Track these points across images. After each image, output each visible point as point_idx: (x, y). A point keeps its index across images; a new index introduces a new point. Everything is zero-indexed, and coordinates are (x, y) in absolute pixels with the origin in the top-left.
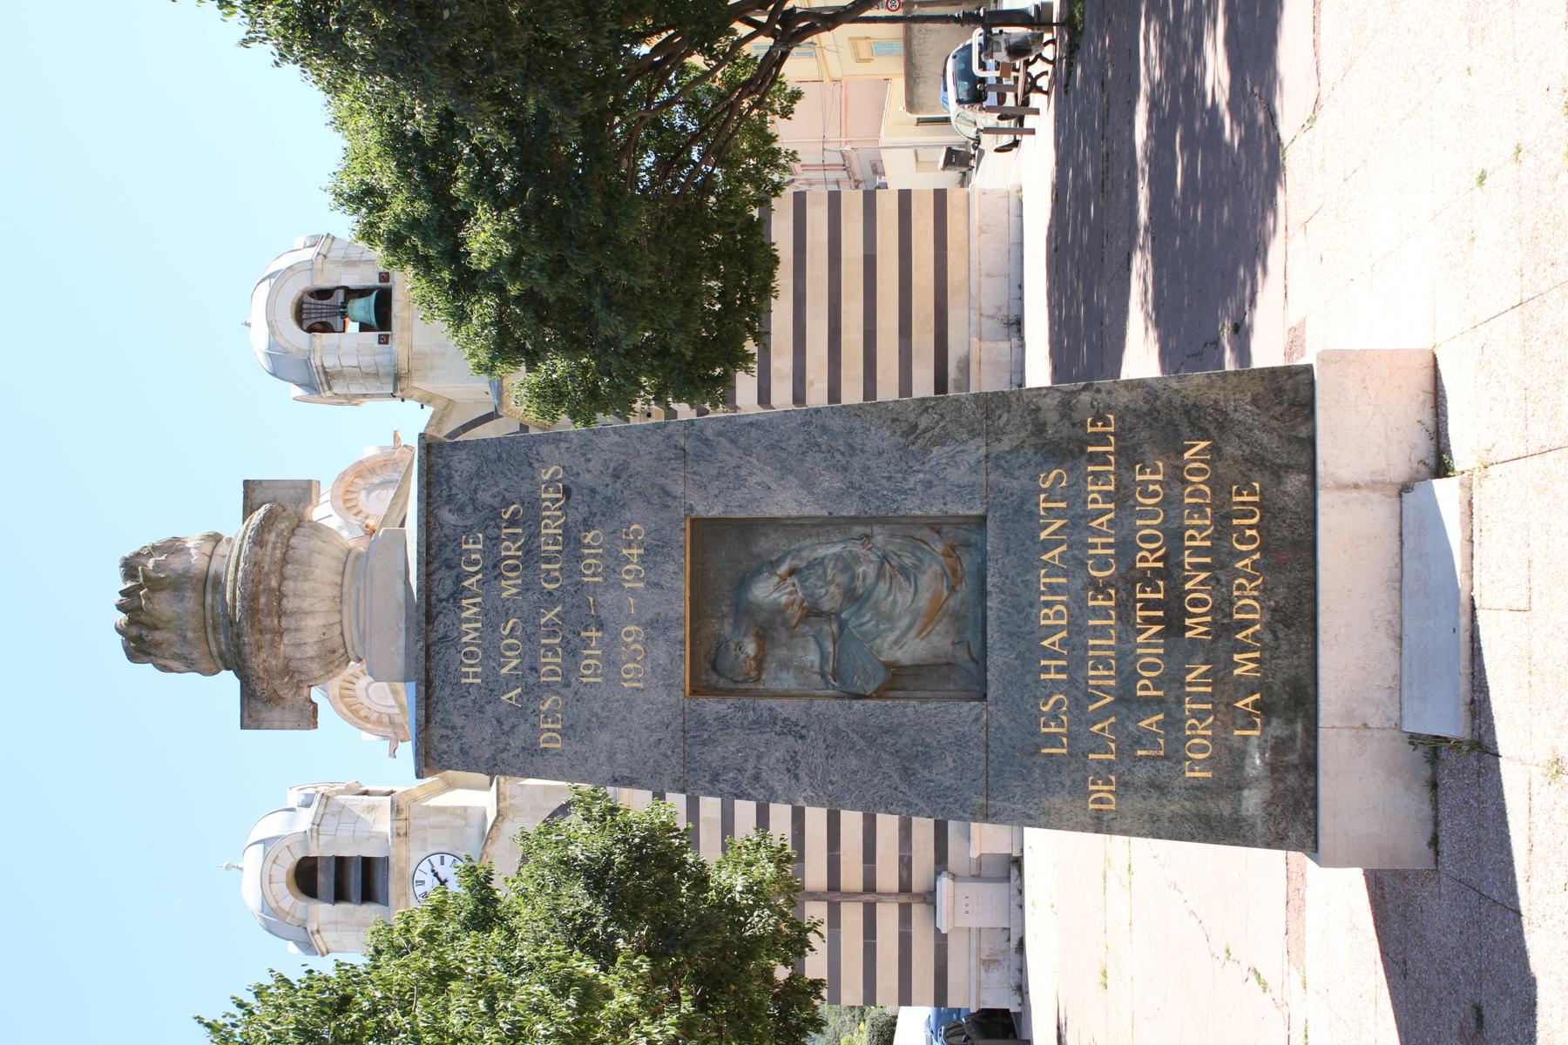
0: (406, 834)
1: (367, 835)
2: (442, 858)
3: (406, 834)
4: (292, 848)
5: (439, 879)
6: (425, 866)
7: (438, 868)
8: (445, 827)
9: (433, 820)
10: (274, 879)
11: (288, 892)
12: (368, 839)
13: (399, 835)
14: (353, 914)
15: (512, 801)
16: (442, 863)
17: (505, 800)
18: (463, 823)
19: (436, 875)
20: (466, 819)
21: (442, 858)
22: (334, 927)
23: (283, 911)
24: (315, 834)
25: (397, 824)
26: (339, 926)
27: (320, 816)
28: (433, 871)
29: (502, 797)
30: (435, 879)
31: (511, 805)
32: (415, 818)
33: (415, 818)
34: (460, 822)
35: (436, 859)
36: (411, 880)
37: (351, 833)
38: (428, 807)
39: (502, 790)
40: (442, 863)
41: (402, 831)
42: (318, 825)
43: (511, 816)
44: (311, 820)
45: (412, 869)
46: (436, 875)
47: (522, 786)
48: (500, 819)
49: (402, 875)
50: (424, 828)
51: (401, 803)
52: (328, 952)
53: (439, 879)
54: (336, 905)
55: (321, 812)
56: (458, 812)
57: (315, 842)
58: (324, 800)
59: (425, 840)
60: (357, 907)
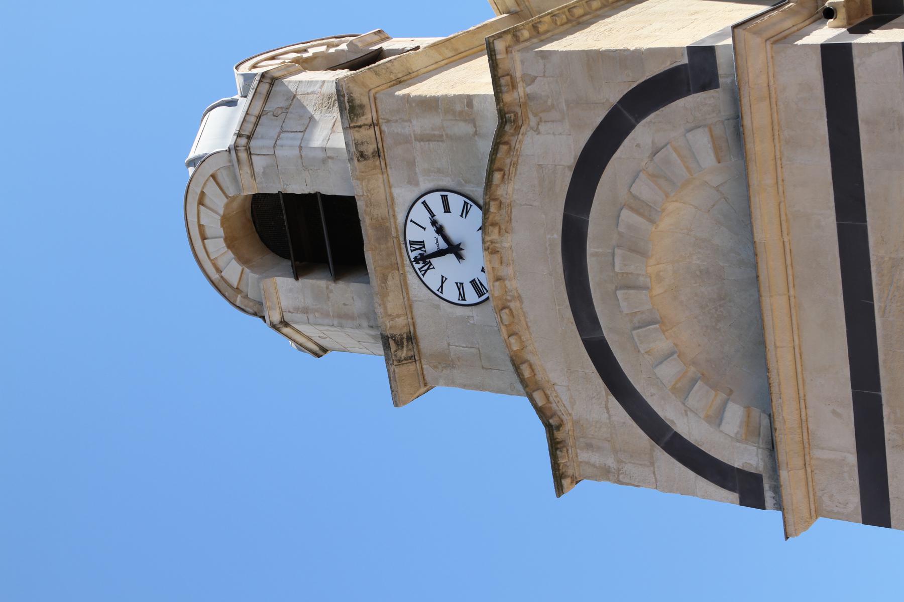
0: (378, 153)
1: (321, 155)
2: (445, 199)
3: (378, 153)
4: (220, 178)
5: (446, 239)
6: (419, 214)
7: (441, 217)
8: (439, 139)
9: (421, 124)
10: (208, 233)
11: (230, 254)
12: (324, 161)
13: (362, 156)
14: (328, 297)
15: (529, 90)
16: (447, 209)
17: (513, 86)
18: (469, 129)
19: (440, 230)
20: (473, 122)
21: (445, 199)
22: (304, 317)
23: (231, 286)
24: (243, 155)
25: (358, 135)
26: (311, 316)
27: (253, 119)
28: (434, 223)
29: (503, 81)
30: (440, 239)
31: (528, 97)
32: (388, 121)
33: (388, 121)
34: (462, 128)
35: (434, 200)
36: (402, 239)
37: (297, 152)
38: (407, 97)
39: (503, 66)
40: (447, 209)
41: (370, 149)
42: (249, 138)
43: (533, 121)
44: (235, 127)
45: (401, 218)
46: (440, 230)
47: (545, 55)
48: (508, 128)
49: (383, 229)
50: (406, 140)
51: (356, 95)
52: (325, 350)
53: (446, 239)
54: (303, 281)
55: (256, 111)
56: (458, 108)
57: (246, 169)
58: (265, 87)
59: (411, 164)
60: (332, 285)
